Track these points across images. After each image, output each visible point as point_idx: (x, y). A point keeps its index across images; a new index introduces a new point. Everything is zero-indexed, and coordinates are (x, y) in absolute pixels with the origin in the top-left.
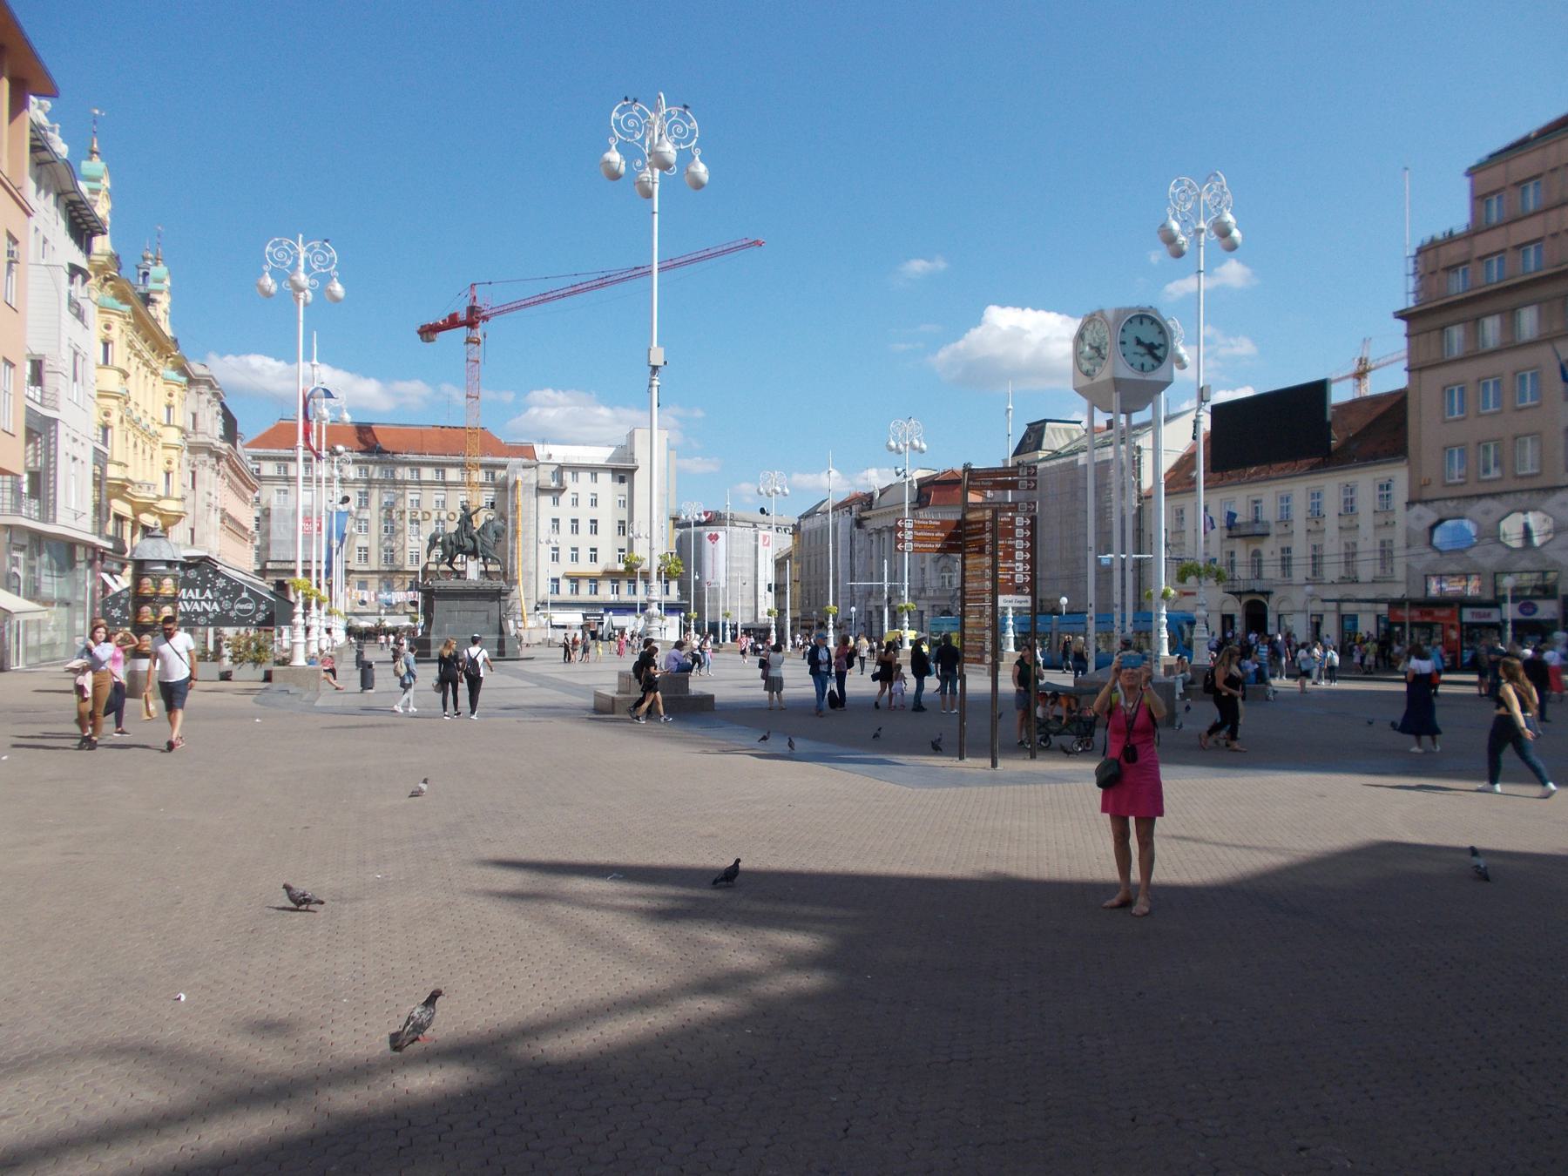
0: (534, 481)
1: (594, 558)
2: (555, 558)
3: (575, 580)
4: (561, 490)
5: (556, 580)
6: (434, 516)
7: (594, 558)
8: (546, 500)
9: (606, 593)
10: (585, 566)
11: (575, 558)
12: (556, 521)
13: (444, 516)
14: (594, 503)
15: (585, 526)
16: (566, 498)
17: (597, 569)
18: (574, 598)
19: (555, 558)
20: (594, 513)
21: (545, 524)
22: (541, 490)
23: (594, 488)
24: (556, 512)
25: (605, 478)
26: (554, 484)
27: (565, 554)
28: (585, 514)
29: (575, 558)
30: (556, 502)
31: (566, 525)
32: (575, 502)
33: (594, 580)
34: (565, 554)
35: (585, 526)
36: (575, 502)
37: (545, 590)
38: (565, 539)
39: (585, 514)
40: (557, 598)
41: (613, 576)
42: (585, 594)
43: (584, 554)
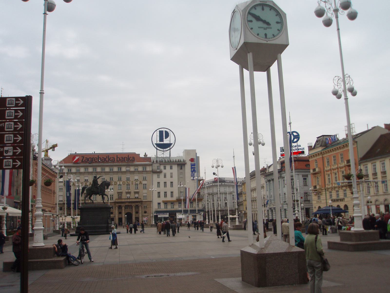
0: (151, 170)
1: (172, 196)
2: (159, 196)
3: (166, 203)
4: (161, 172)
5: (159, 204)
6: (118, 183)
7: (172, 196)
8: (155, 176)
9: (176, 207)
10: (169, 198)
11: (165, 195)
12: (159, 183)
13: (121, 183)
14: (171, 177)
15: (168, 184)
16: (162, 175)
17: (174, 199)
18: (166, 209)
19: (159, 196)
20: (171, 180)
21: (155, 184)
22: (154, 172)
23: (171, 171)
24: (158, 180)
25: (175, 167)
26: (158, 170)
27: (162, 194)
28: (168, 180)
29: (165, 195)
30: (158, 177)
31: (162, 184)
32: (165, 176)
33: (172, 203)
34: (162, 194)
35: (168, 184)
36: (165, 176)
37: (155, 207)
38: (162, 189)
39: (168, 180)
40: (159, 210)
41: (179, 201)
42: (169, 208)
43: (169, 194)
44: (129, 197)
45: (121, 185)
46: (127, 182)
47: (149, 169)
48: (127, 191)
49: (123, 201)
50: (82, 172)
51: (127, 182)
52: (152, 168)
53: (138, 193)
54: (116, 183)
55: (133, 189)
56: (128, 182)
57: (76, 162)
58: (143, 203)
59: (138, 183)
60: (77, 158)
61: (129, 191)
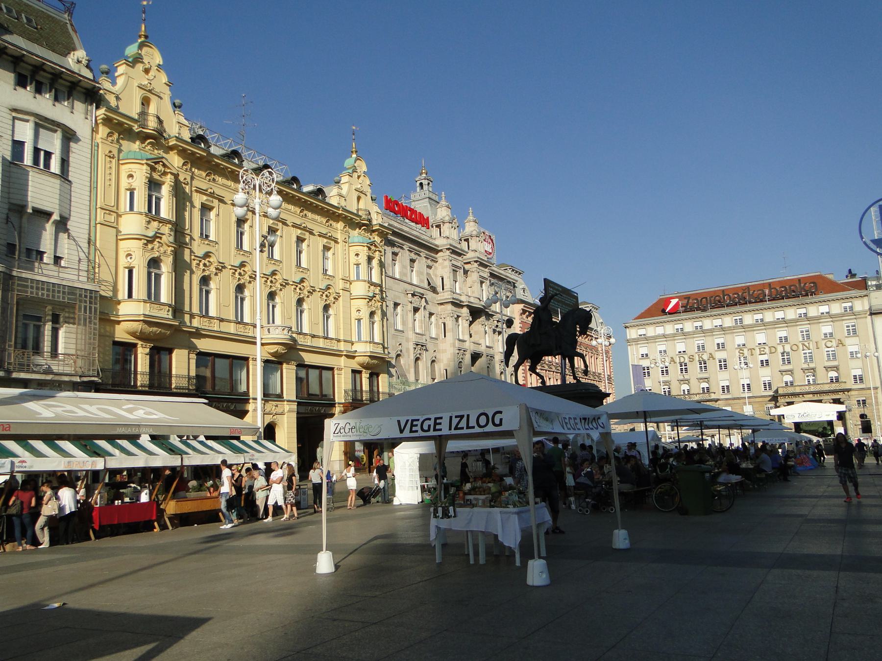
0: (867, 308)
6: (780, 349)
13: (788, 348)
44: (814, 380)
45: (788, 354)
46: (803, 345)
47: (860, 305)
48: (805, 366)
49: (798, 390)
50: (689, 332)
51: (803, 345)
52: (870, 303)
53: (836, 368)
54: (773, 350)
55: (821, 361)
56: (806, 344)
57: (674, 312)
58: (852, 393)
59: (834, 343)
60: (674, 302)
61: (812, 365)
